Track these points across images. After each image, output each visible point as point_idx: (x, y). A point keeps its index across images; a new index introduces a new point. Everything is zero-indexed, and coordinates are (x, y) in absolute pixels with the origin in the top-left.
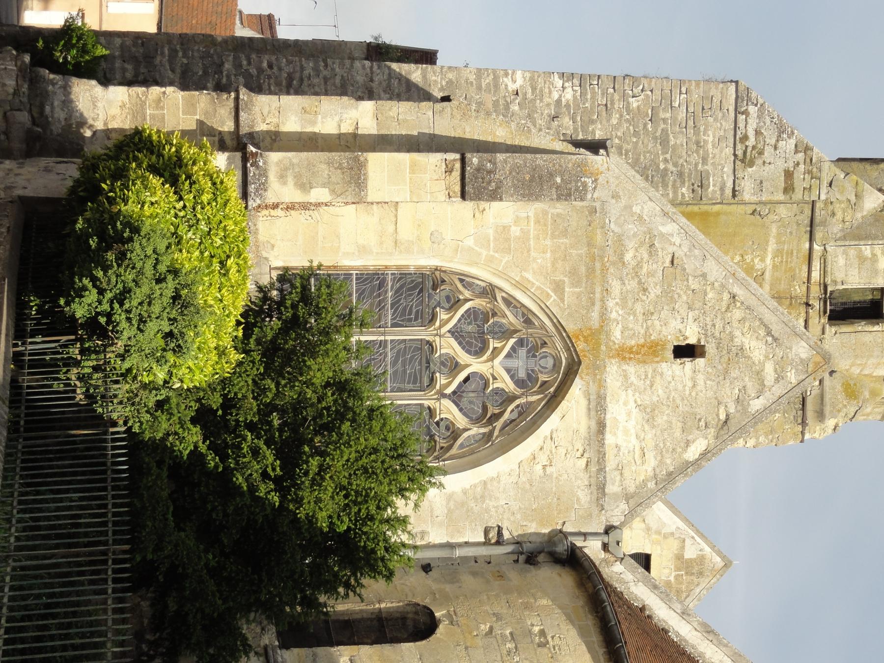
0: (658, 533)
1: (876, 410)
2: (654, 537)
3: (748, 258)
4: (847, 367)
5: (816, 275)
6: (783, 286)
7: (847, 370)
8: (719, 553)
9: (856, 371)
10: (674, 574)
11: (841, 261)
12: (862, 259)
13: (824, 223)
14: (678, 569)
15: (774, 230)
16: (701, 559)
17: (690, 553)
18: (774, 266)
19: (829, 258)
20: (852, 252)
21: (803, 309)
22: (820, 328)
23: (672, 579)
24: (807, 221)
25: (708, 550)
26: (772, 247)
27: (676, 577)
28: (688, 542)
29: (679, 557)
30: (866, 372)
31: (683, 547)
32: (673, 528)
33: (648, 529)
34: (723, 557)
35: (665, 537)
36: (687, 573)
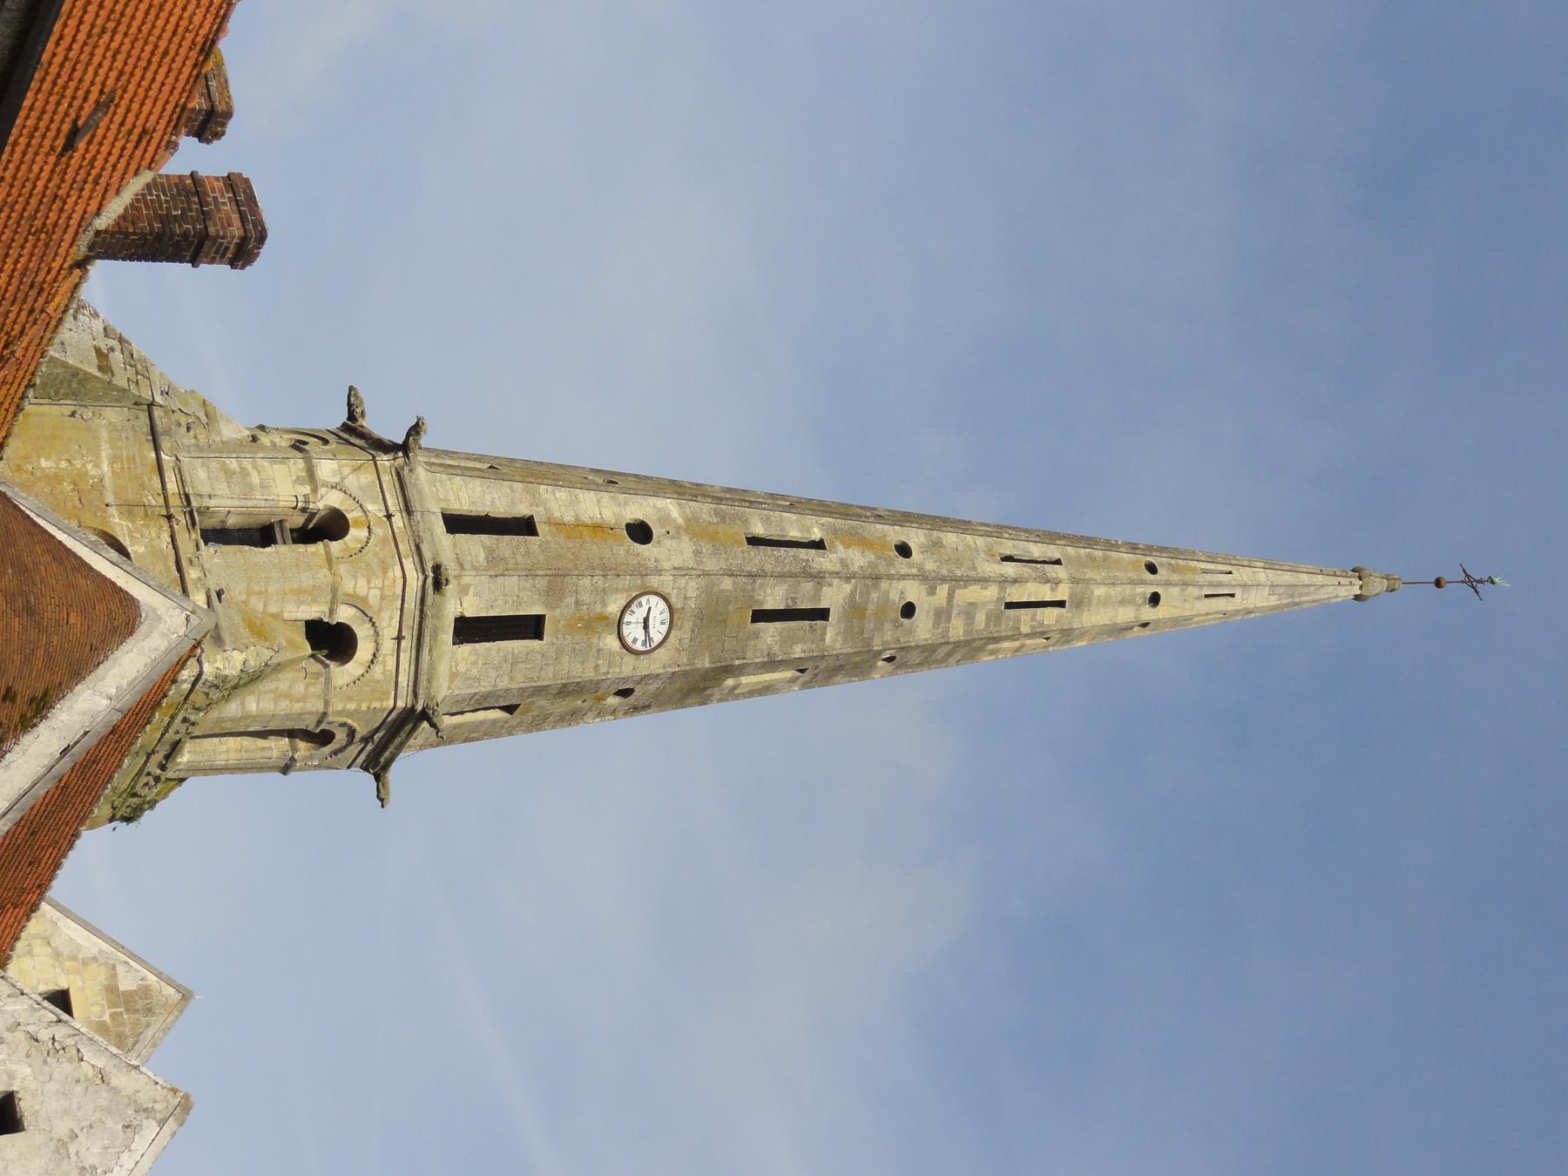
0: (73, 958)
1: (312, 689)
2: (68, 963)
3: (78, 464)
4: (244, 597)
5: (172, 486)
6: (131, 495)
7: (245, 602)
8: (170, 982)
9: (257, 604)
10: (108, 1012)
11: (202, 474)
12: (229, 474)
13: (168, 433)
14: (112, 1005)
15: (104, 435)
16: (146, 991)
17: (126, 983)
18: (114, 473)
19: (185, 468)
20: (213, 465)
21: (164, 522)
22: (192, 544)
23: (107, 1018)
24: (147, 429)
25: (152, 978)
26: (105, 452)
27: (113, 1016)
28: (120, 969)
29: (111, 989)
30: (273, 609)
31: (115, 976)
32: (95, 951)
33: (57, 955)
34: (178, 988)
35: (85, 962)
36: (127, 1010)
